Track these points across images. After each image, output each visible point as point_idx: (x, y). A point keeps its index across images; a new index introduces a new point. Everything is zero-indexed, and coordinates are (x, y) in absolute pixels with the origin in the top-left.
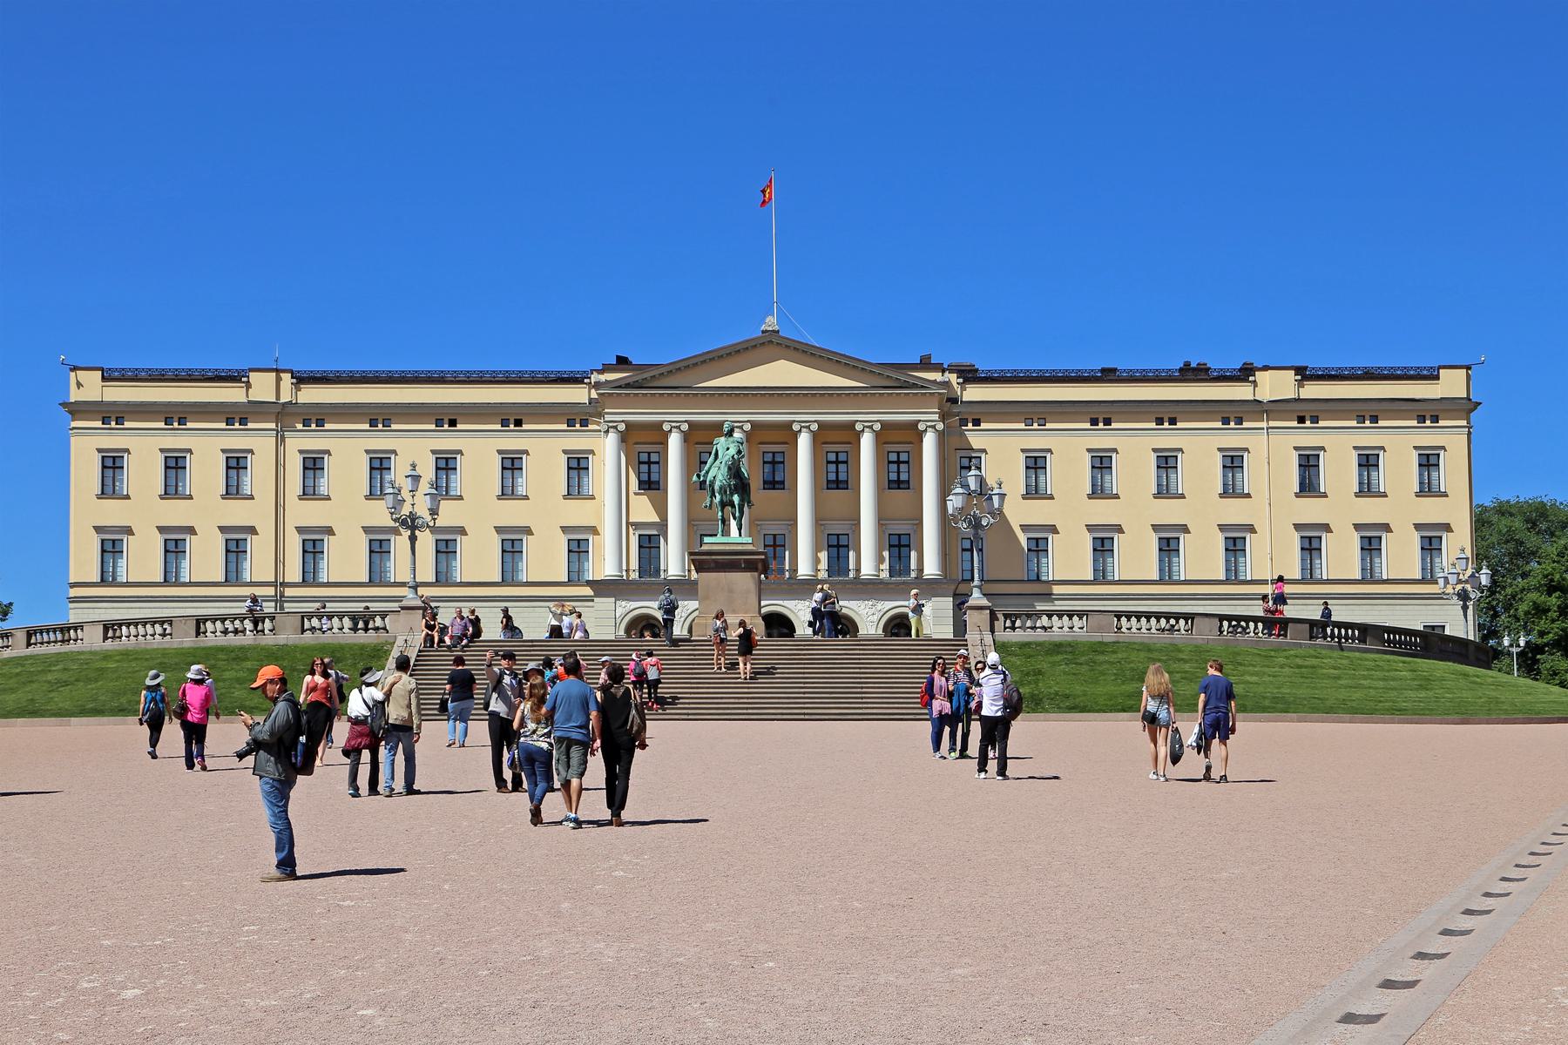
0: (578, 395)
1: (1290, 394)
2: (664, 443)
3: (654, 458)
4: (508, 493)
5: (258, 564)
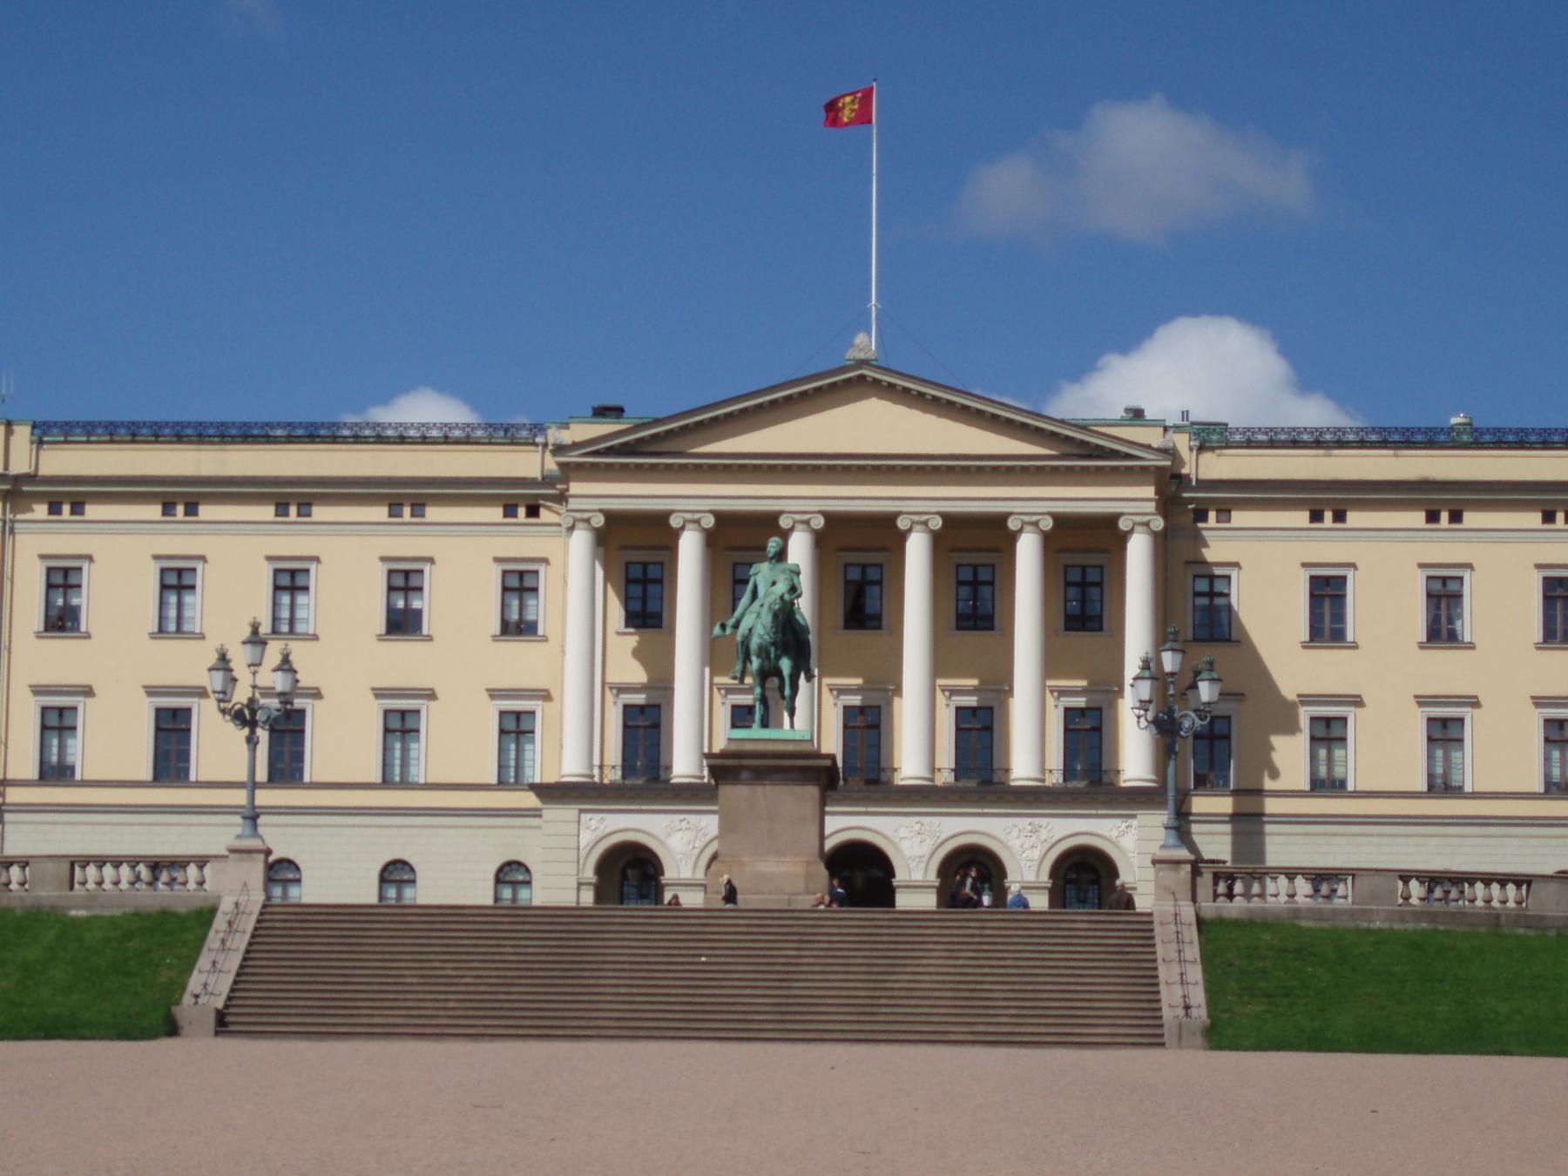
0: (526, 463)
2: (671, 548)
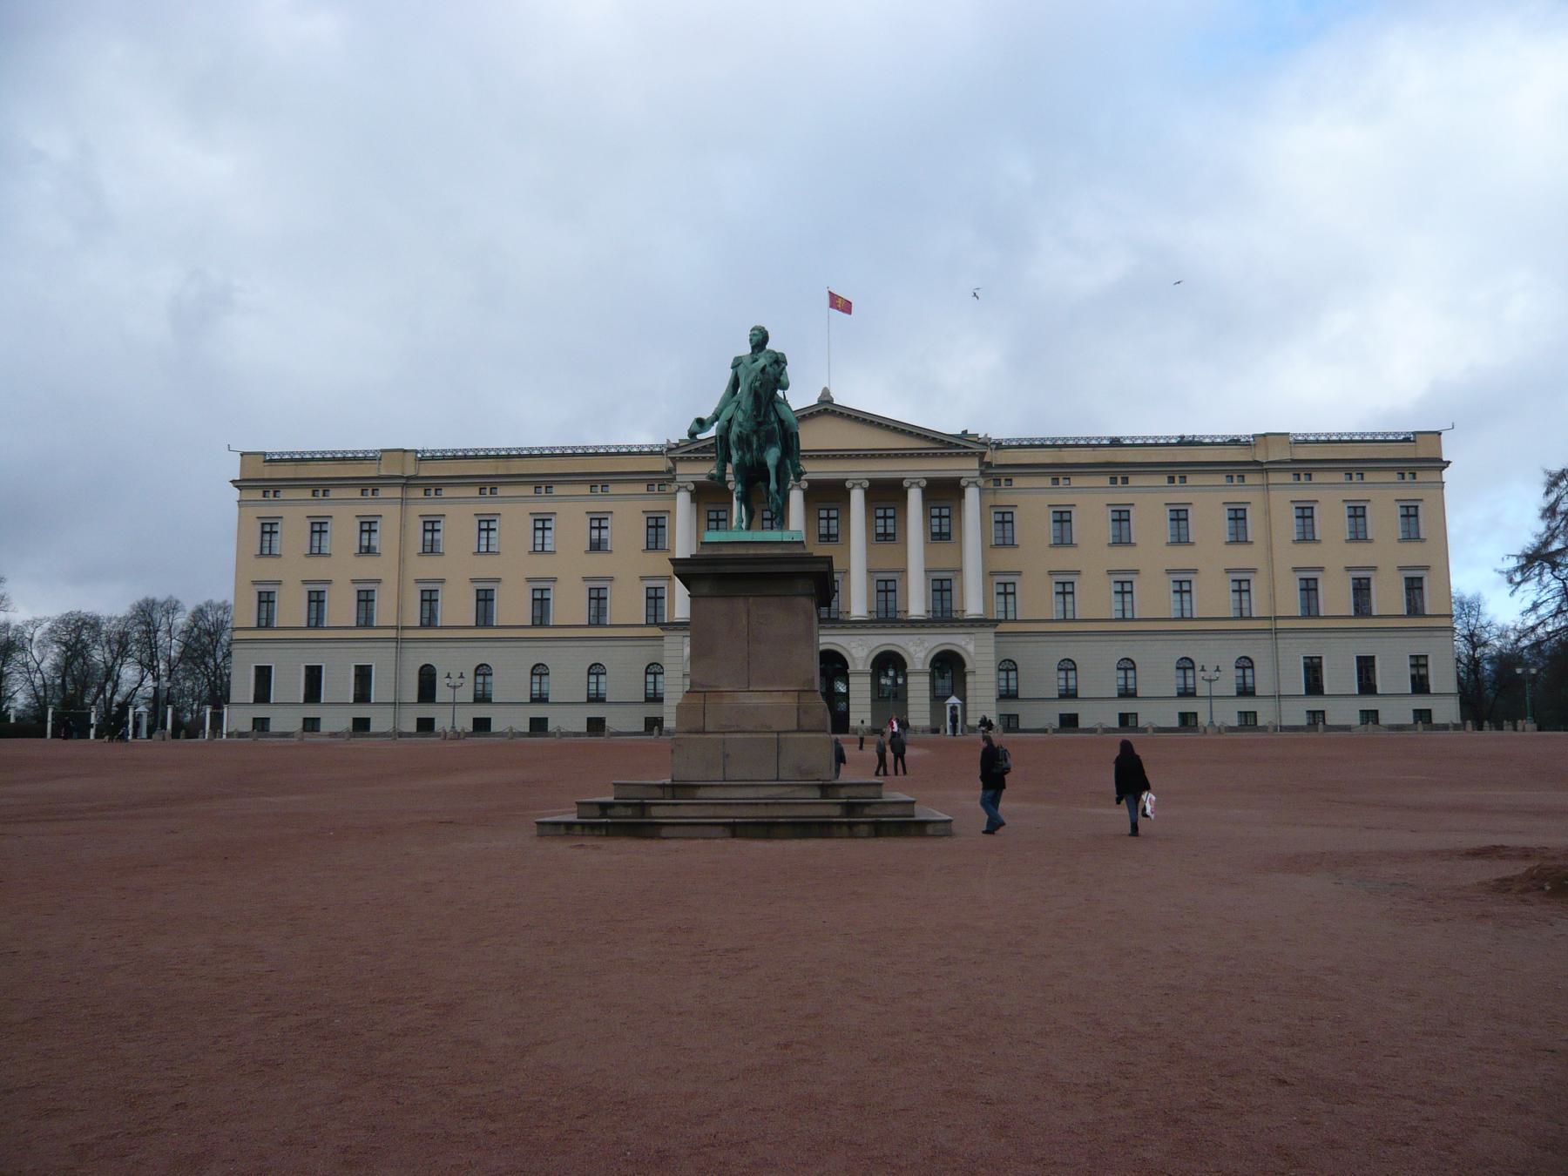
1: (1287, 456)
3: (722, 515)
4: (597, 546)
5: (384, 612)
